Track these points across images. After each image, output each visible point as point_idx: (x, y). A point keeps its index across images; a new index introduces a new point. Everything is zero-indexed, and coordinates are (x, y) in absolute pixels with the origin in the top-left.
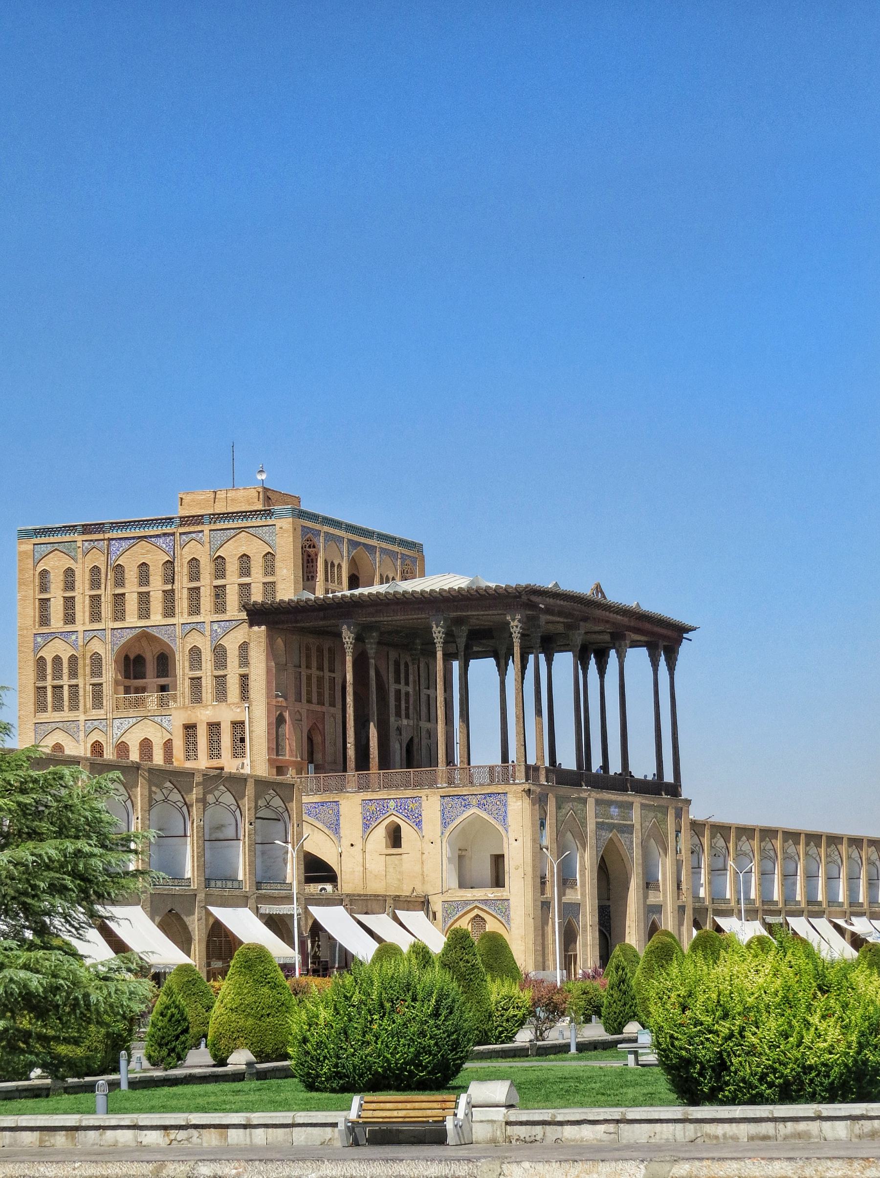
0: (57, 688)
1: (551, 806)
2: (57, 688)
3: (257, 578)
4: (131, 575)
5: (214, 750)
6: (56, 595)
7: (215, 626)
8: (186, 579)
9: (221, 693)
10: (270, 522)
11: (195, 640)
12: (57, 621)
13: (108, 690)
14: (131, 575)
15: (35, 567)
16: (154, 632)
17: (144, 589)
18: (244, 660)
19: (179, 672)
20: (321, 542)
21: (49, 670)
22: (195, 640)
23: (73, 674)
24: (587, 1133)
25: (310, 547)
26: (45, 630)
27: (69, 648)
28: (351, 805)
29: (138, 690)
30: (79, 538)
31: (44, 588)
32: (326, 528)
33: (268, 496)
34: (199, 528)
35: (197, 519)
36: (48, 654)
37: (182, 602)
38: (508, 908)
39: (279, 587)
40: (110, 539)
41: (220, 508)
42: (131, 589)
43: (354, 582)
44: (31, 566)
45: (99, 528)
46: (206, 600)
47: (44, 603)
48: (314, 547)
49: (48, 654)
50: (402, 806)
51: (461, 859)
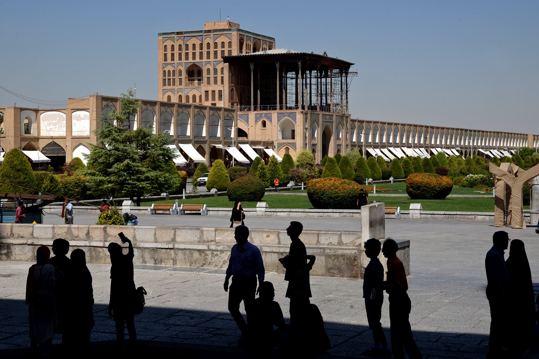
0: (169, 79)
1: (309, 116)
2: (169, 79)
3: (226, 49)
4: (190, 47)
5: (214, 98)
8: (206, 48)
9: (216, 82)
11: (208, 66)
13: (183, 80)
14: (190, 47)
15: (163, 43)
16: (197, 64)
17: (194, 51)
18: (222, 73)
19: (204, 75)
21: (167, 74)
22: (208, 66)
23: (174, 75)
24: (283, 214)
26: (166, 62)
28: (252, 115)
31: (165, 50)
32: (247, 34)
33: (230, 24)
35: (209, 31)
39: (233, 51)
41: (216, 27)
42: (190, 51)
45: (181, 33)
46: (212, 55)
47: (165, 55)
49: (167, 69)
50: (266, 115)
51: (283, 131)
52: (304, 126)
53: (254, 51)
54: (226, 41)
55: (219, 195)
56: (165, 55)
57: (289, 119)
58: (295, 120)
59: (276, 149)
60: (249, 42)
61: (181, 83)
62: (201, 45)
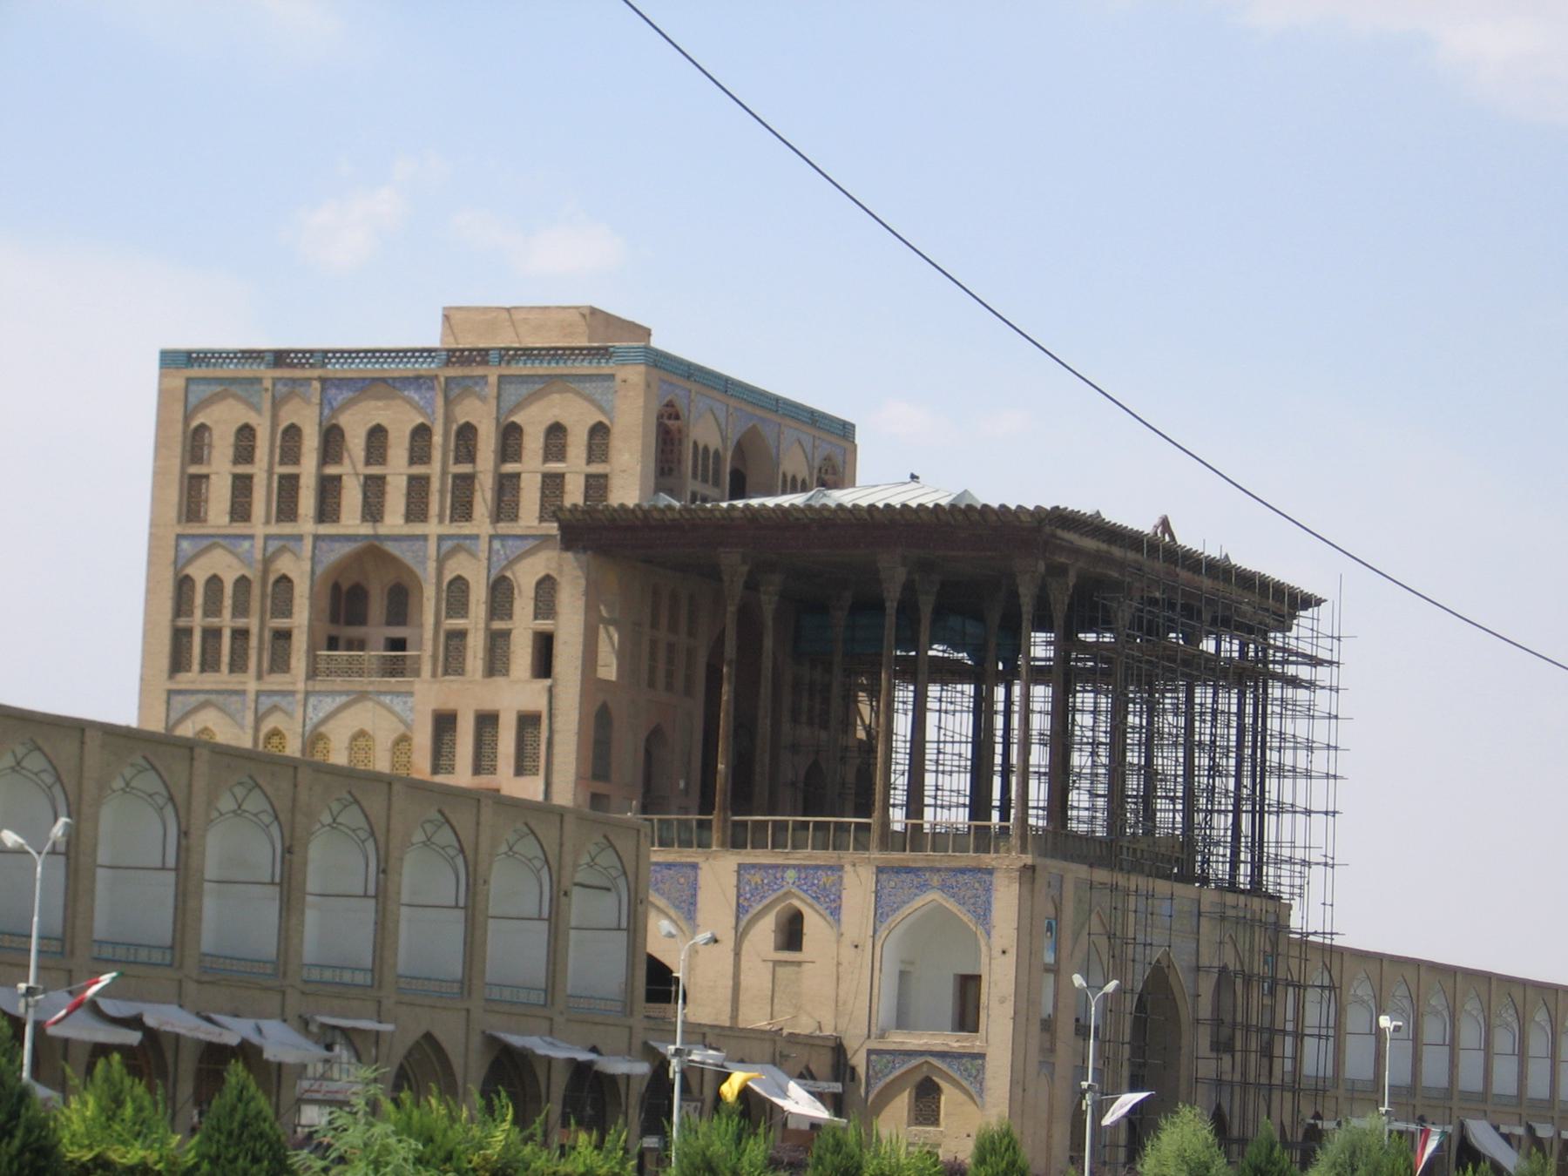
0: (212, 635)
2: (212, 635)
6: (220, 469)
7: (497, 545)
10: (605, 368)
13: (300, 642)
16: (390, 547)
17: (375, 470)
19: (429, 618)
21: (199, 599)
22: (459, 566)
23: (241, 609)
25: (669, 418)
26: (194, 529)
27: (235, 562)
28: (719, 872)
29: (351, 645)
30: (267, 374)
34: (478, 371)
38: (981, 1069)
40: (323, 380)
42: (352, 470)
44: (180, 416)
48: (677, 417)
49: (199, 573)
53: (738, 491)
54: (577, 416)
57: (951, 905)
58: (983, 914)
61: (280, 662)
62: (421, 433)
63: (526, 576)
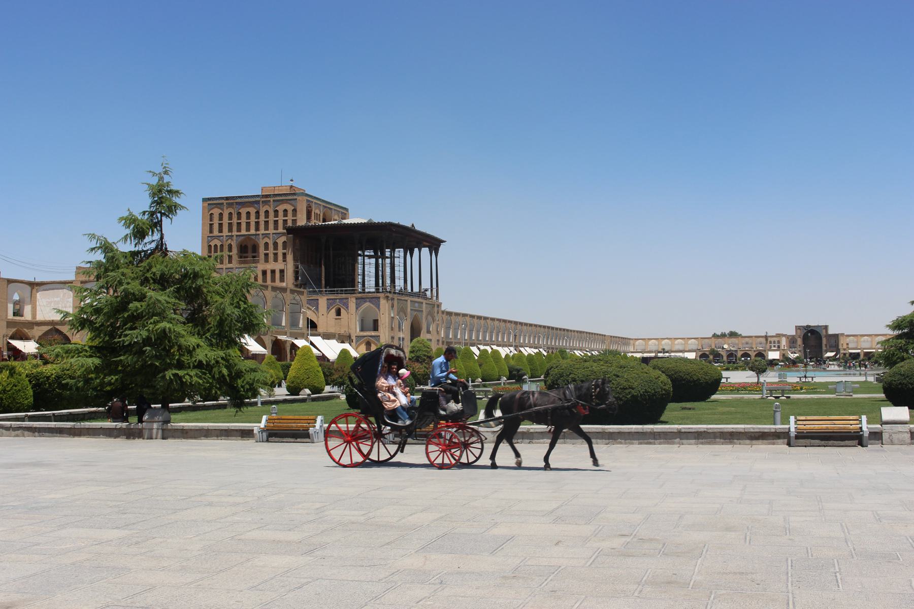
1: (396, 302)
3: (290, 218)
5: (273, 280)
6: (216, 222)
9: (276, 260)
10: (295, 197)
12: (216, 233)
20: (313, 206)
28: (323, 301)
30: (225, 202)
36: (212, 244)
37: (262, 226)
42: (244, 220)
43: (324, 221)
47: (211, 225)
49: (212, 244)
52: (389, 314)
53: (324, 221)
55: (314, 400)
56: (211, 225)
59: (354, 344)
60: (317, 211)
61: (230, 262)
63: (280, 241)
